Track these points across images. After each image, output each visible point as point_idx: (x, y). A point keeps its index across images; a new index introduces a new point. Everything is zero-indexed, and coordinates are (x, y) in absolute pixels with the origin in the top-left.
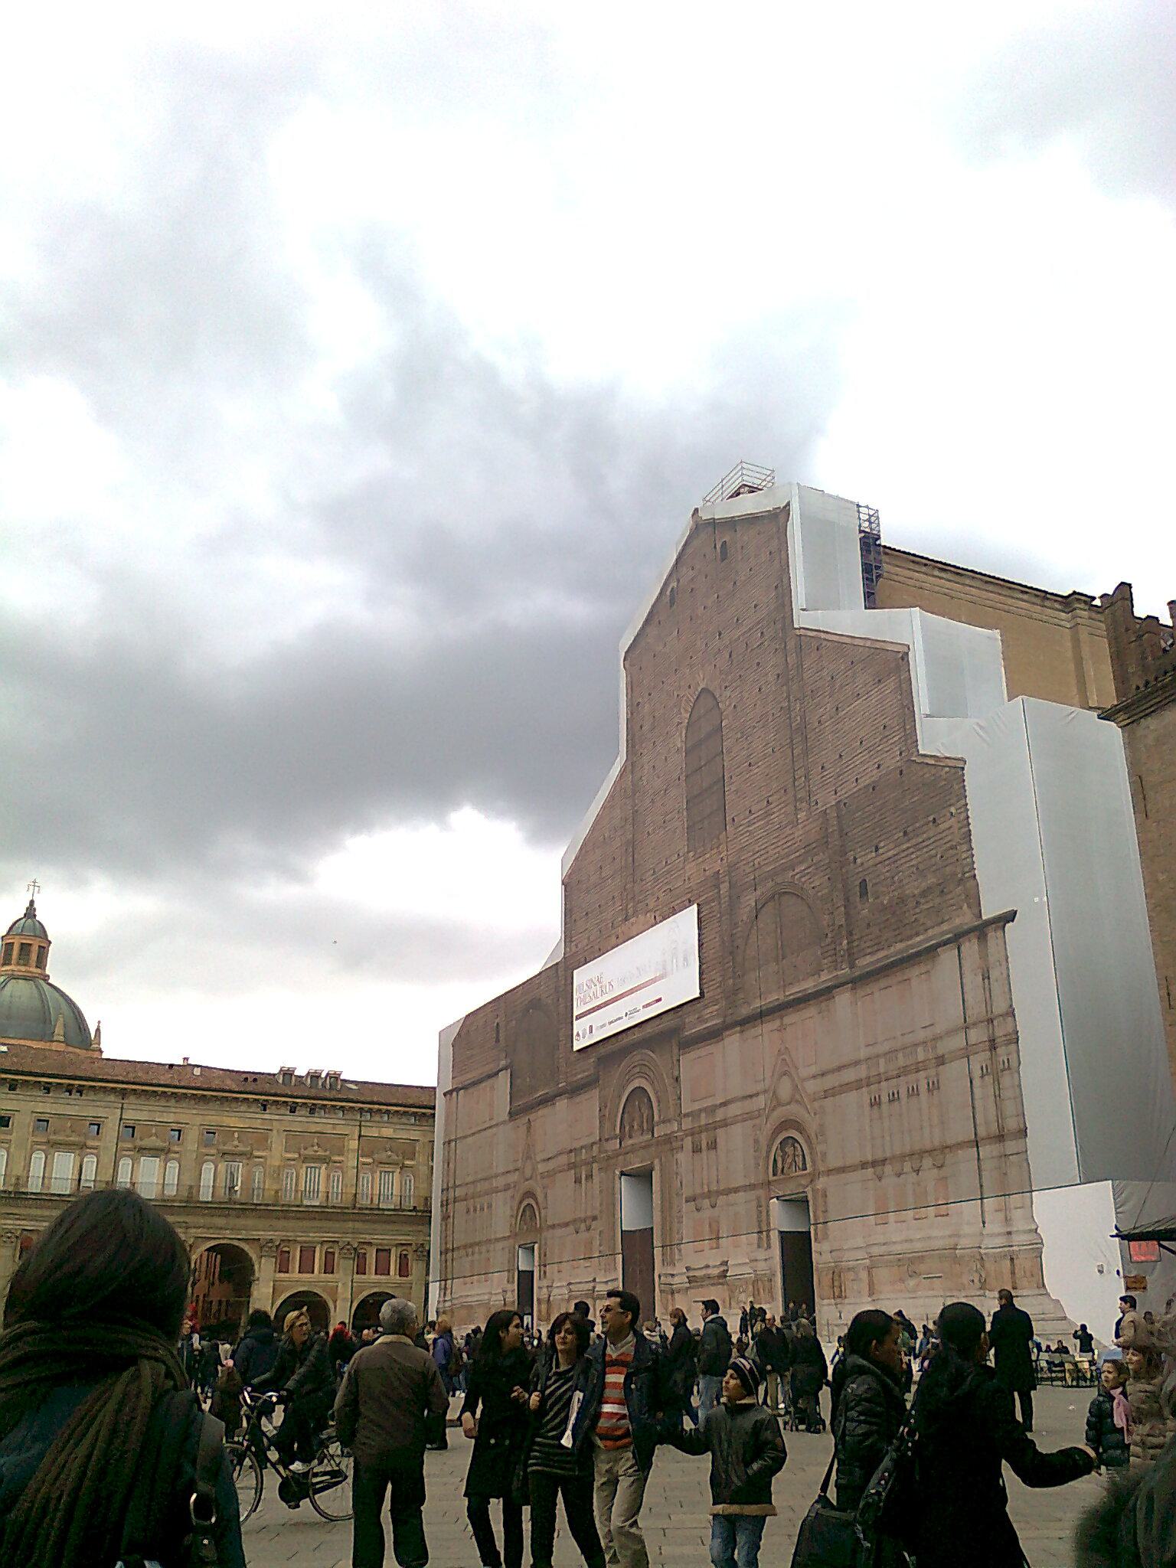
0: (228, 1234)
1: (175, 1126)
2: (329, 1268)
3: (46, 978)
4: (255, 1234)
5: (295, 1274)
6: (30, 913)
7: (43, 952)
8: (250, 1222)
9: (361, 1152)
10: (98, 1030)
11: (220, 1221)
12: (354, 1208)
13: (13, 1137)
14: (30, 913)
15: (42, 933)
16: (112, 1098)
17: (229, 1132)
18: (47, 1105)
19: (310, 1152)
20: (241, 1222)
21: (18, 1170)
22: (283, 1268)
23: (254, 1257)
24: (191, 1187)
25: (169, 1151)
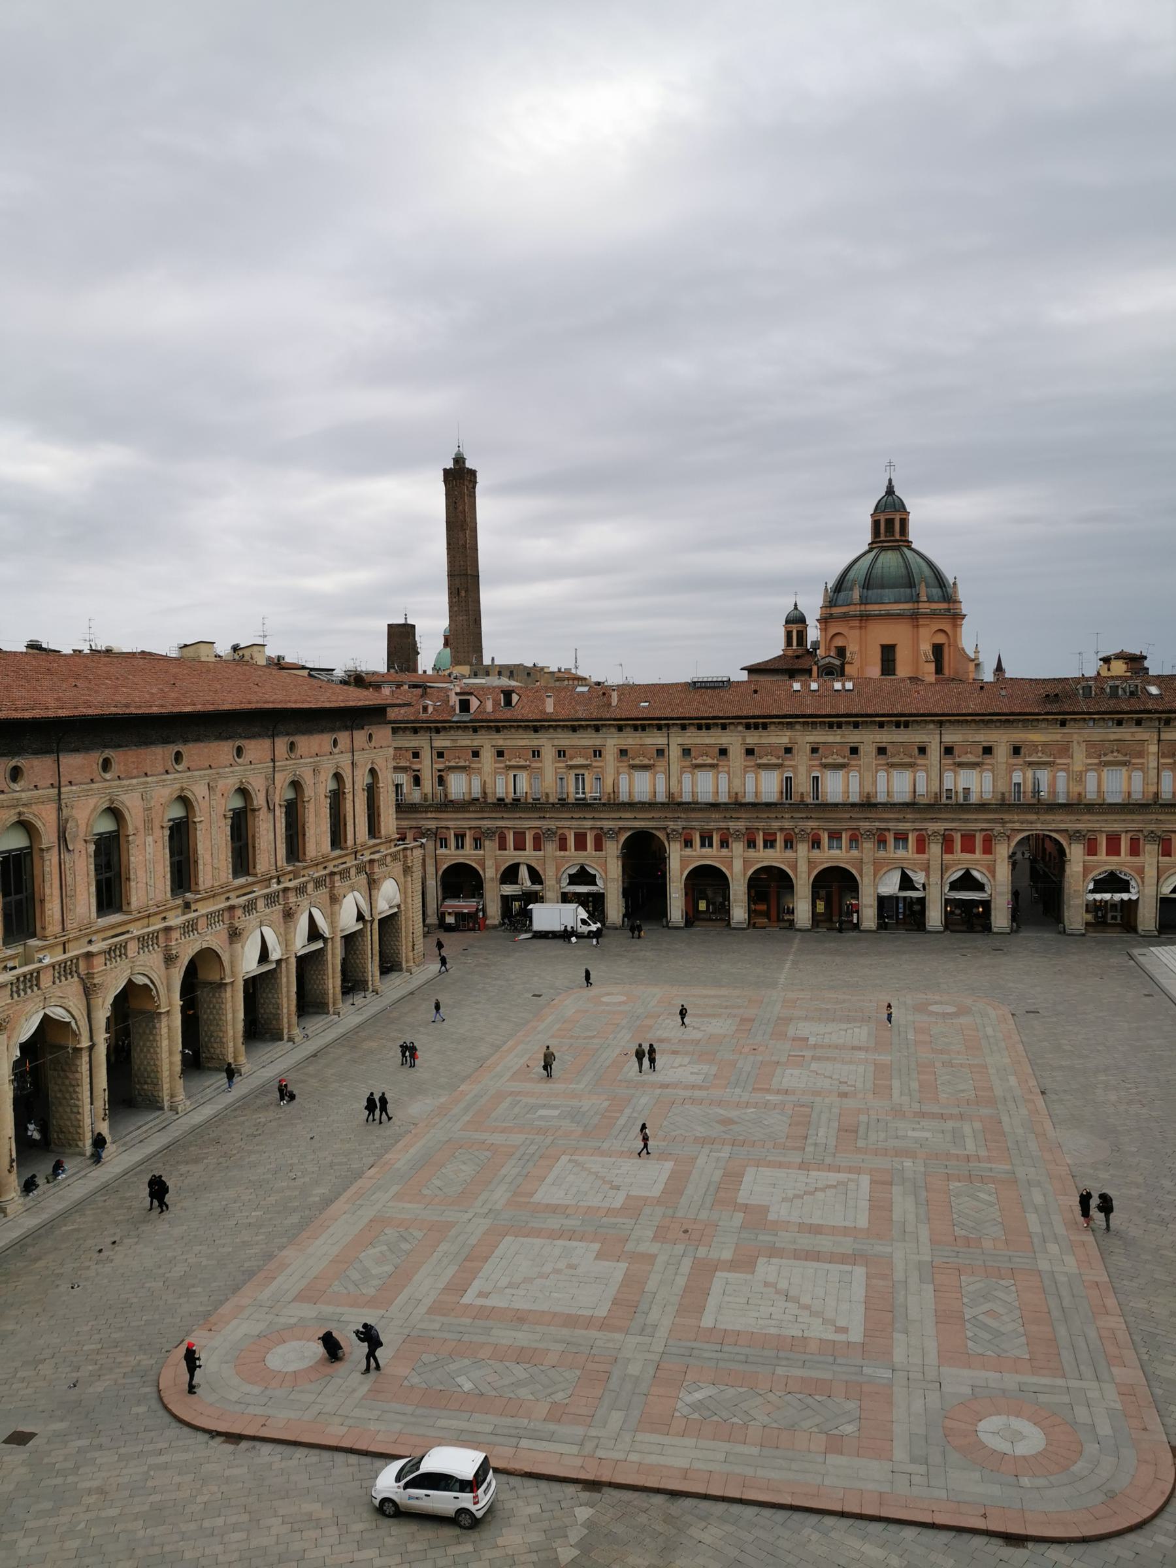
0: (1039, 826)
1: (985, 744)
2: (1135, 850)
3: (908, 545)
4: (1063, 826)
5: (1102, 856)
6: (890, 491)
7: (904, 523)
8: (1058, 818)
9: (1160, 754)
10: (955, 584)
11: (1034, 817)
12: (1155, 804)
13: (861, 762)
14: (890, 491)
15: (900, 507)
16: (932, 726)
17: (1034, 747)
18: (885, 737)
19: (1109, 758)
20: (1049, 817)
21: (868, 788)
22: (1092, 850)
23: (1064, 844)
24: (1003, 794)
25: (983, 764)
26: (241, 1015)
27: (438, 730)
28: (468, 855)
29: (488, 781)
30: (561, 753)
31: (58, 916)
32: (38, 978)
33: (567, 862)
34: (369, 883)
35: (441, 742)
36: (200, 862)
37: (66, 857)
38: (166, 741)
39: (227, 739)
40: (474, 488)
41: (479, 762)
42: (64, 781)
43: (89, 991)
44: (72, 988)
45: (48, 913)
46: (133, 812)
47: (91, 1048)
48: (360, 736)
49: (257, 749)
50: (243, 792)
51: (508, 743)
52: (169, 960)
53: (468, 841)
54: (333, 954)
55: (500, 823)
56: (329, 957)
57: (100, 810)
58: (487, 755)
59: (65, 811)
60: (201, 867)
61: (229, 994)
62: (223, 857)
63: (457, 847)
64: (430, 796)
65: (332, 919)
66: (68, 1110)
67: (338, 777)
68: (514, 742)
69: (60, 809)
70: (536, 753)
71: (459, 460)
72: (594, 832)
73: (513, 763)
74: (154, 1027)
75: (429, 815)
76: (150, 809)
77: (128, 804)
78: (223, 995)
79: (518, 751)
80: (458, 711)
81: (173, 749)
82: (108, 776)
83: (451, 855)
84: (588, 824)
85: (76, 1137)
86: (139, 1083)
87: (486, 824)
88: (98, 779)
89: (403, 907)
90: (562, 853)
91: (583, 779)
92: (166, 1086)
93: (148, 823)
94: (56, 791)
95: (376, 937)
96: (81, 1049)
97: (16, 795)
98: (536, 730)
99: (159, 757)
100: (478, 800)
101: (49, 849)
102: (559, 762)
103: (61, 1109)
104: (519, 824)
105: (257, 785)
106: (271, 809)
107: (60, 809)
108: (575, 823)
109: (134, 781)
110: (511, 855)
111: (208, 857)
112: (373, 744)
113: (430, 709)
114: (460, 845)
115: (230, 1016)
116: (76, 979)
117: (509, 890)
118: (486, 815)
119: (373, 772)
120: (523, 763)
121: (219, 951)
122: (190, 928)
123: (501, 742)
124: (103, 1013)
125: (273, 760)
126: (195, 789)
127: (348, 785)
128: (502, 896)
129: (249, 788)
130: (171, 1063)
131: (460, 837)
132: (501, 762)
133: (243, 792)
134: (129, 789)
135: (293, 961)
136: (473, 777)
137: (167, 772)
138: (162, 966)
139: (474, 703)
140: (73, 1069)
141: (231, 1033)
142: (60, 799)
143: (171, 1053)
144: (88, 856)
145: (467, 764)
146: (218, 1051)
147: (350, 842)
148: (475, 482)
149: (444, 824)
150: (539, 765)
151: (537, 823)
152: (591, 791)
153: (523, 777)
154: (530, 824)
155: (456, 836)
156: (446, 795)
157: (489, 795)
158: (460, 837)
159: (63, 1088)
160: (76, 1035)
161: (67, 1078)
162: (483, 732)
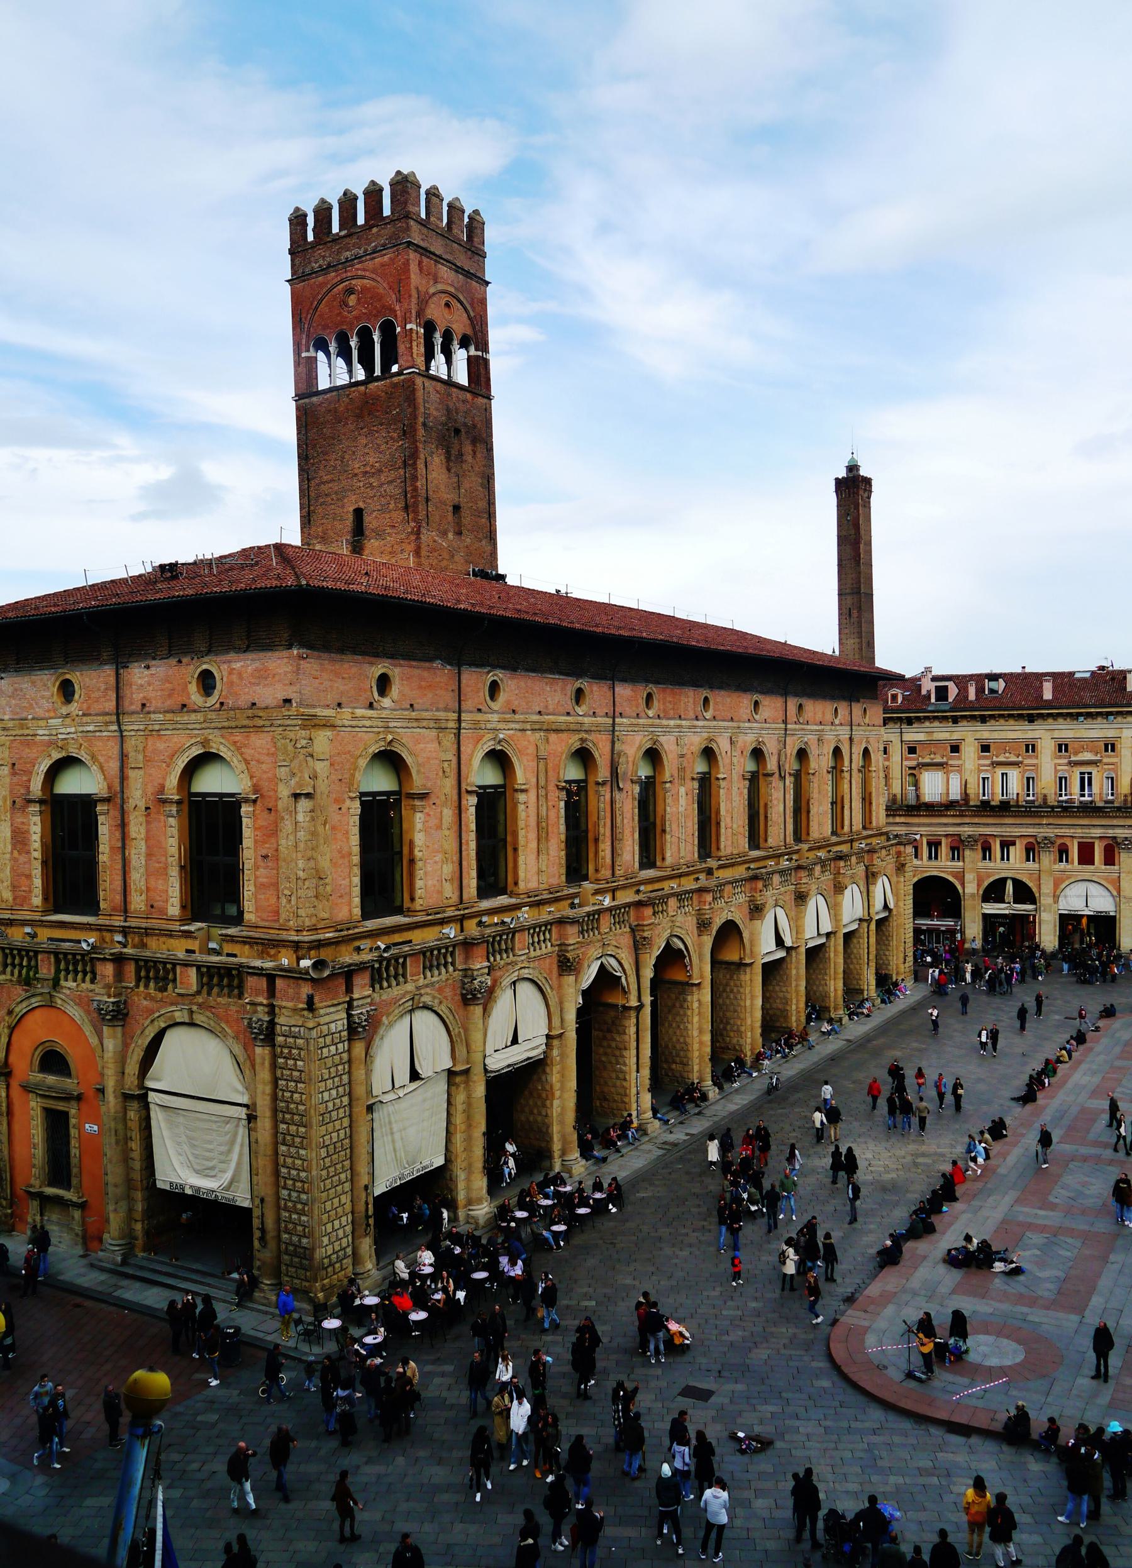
26: (759, 1002)
27: (910, 721)
28: (944, 866)
30: (1063, 747)
31: (608, 860)
32: (598, 920)
33: (1068, 878)
34: (867, 877)
35: (914, 734)
36: (723, 824)
37: (618, 796)
38: (696, 684)
39: (745, 691)
40: (869, 497)
41: (959, 758)
42: (617, 714)
43: (639, 945)
44: (621, 939)
45: (601, 854)
46: (670, 756)
47: (639, 1008)
48: (857, 709)
49: (771, 706)
50: (758, 754)
51: (996, 735)
52: (703, 925)
53: (944, 849)
54: (835, 951)
56: (832, 955)
57: (644, 749)
58: (970, 751)
59: (617, 746)
60: (723, 830)
61: (748, 977)
62: (741, 823)
63: (930, 858)
64: (899, 797)
65: (798, 930)
66: (614, 1075)
67: (837, 752)
68: (1003, 735)
69: (613, 743)
70: (1031, 747)
71: (852, 468)
72: (1105, 843)
73: (1001, 759)
74: (685, 1000)
76: (682, 756)
77: (666, 747)
78: (742, 977)
79: (1005, 745)
80: (933, 700)
81: (705, 693)
82: (651, 713)
83: (924, 866)
84: (1098, 832)
85: (621, 1106)
86: (667, 1061)
87: (966, 831)
88: (642, 714)
89: (894, 912)
90: (1063, 865)
91: (1090, 779)
92: (696, 1068)
93: (682, 769)
94: (610, 721)
95: (873, 940)
96: (630, 1008)
97: (580, 718)
98: (1031, 719)
99: (691, 700)
100: (957, 802)
101: (604, 783)
102: (1060, 757)
103: (605, 1074)
105: (771, 748)
106: (782, 778)
107: (613, 743)
108: (1079, 832)
109: (672, 723)
110: (997, 868)
111: (728, 820)
112: (867, 721)
113: (900, 700)
114: (934, 855)
115: (748, 1003)
116: (628, 929)
117: (992, 908)
118: (967, 820)
119: (866, 752)
120: (1013, 759)
121: (741, 926)
122: (718, 891)
123: (986, 735)
124: (648, 973)
125: (785, 722)
126: (719, 740)
127: (847, 763)
128: (985, 916)
129: (764, 749)
130: (701, 1043)
131: (934, 845)
132: (986, 758)
133: (758, 754)
134: (667, 730)
135: (803, 950)
136: (951, 775)
137: (697, 719)
138: (695, 931)
139: (953, 691)
140: (620, 1029)
141: (749, 1022)
142: (613, 731)
143: (701, 1031)
144: (634, 798)
145: (945, 760)
146: (735, 1041)
147: (846, 829)
148: (871, 491)
150: (1034, 761)
152: (1100, 790)
153: (1014, 775)
154: (1021, 829)
155: (929, 844)
156: (918, 797)
157: (972, 796)
158: (934, 845)
159: (609, 1050)
160: (625, 992)
161: (614, 1040)
162: (965, 723)
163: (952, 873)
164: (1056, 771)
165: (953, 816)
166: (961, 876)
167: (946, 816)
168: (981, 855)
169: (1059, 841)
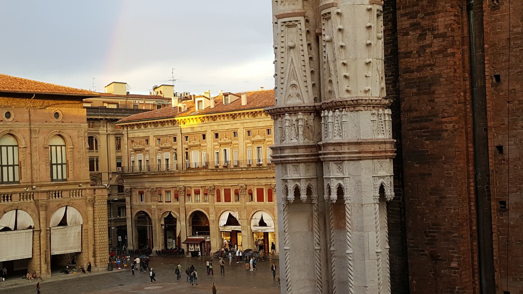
29: (210, 154)
51: (220, 128)
55: (216, 183)
73: (222, 141)
75: (182, 179)
84: (264, 182)
98: (234, 117)
102: (247, 139)
104: (228, 183)
108: (255, 181)
123: (216, 128)
149: (188, 184)
150: (237, 142)
151: (235, 182)
153: (229, 150)
157: (211, 163)
163: (204, 209)
164: (246, 147)
165: (203, 175)
166: (208, 210)
167: (199, 175)
168: (216, 199)
169: (248, 188)
